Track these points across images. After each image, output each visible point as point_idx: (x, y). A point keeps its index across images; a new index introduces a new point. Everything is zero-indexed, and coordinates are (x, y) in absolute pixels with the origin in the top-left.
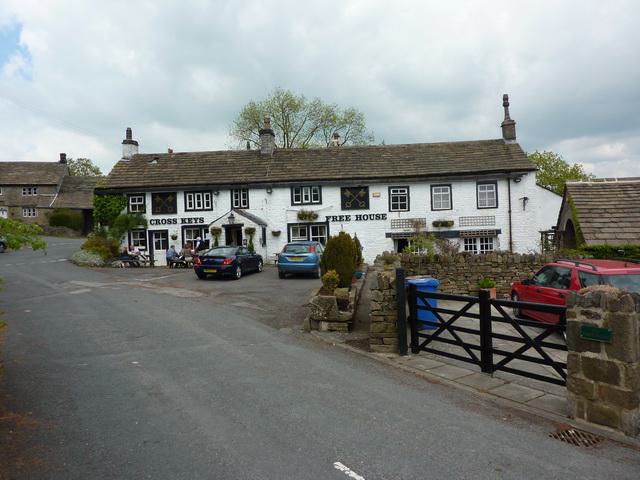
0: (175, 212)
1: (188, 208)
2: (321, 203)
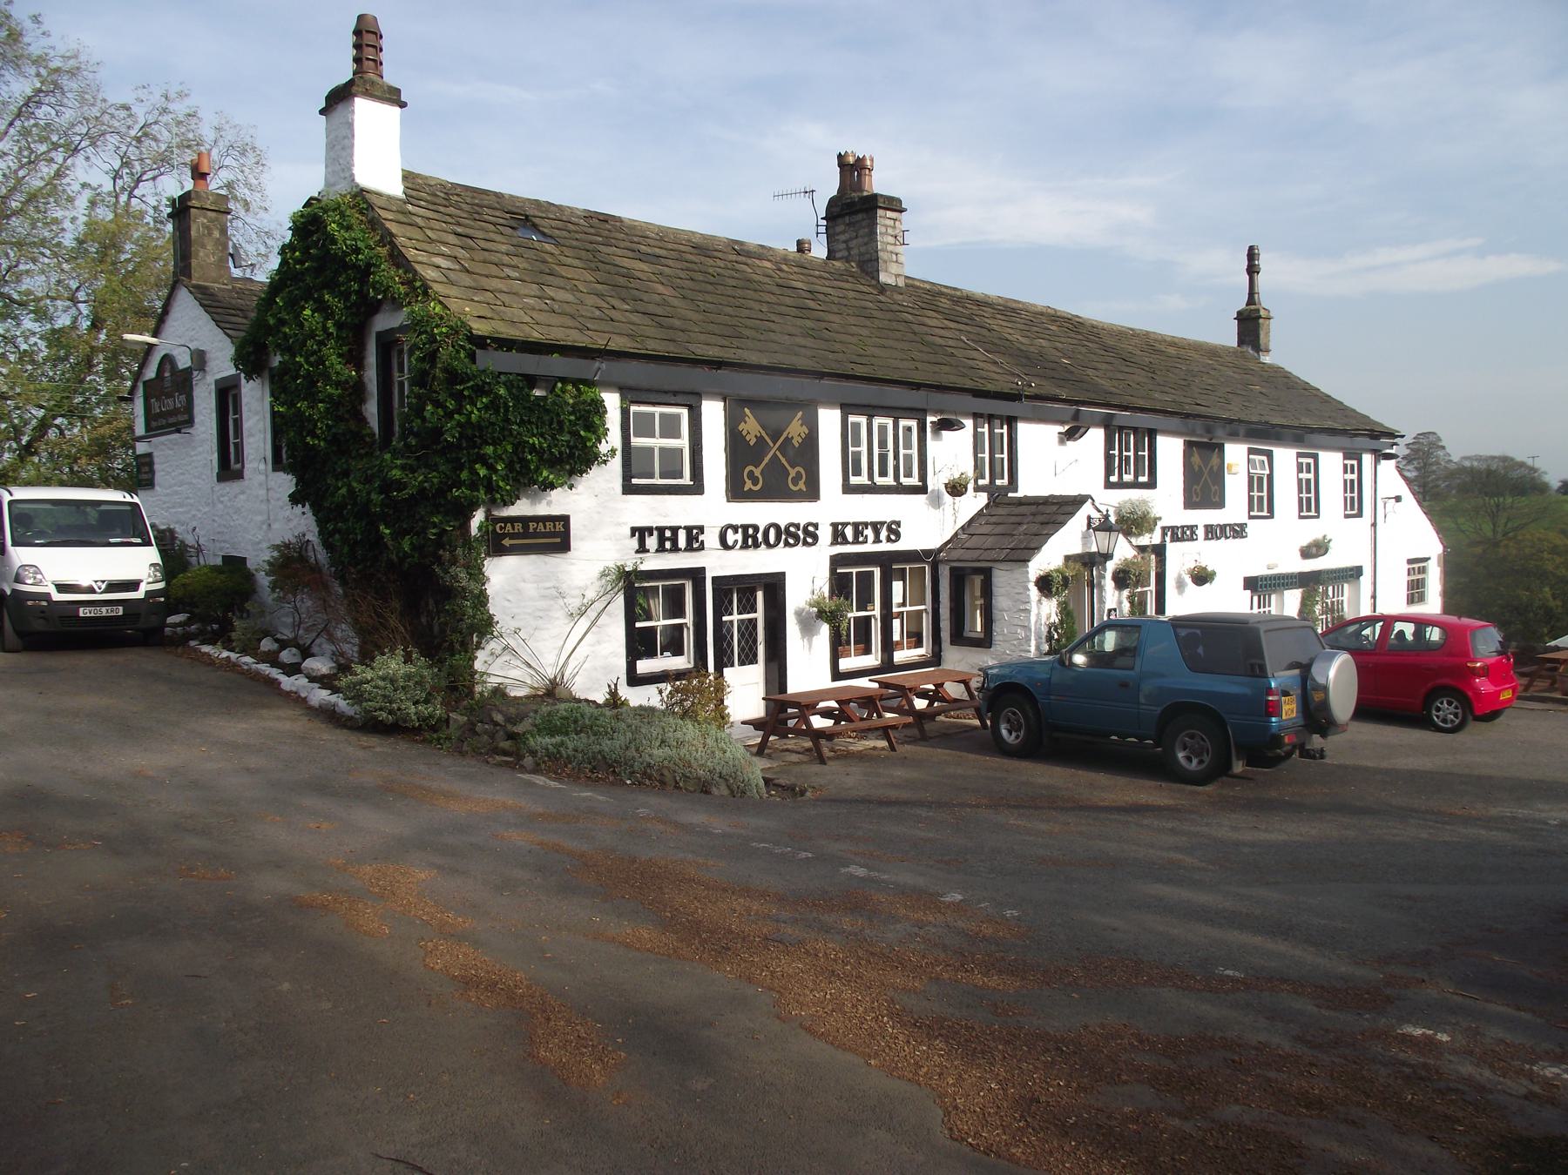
0: (812, 493)
1: (854, 480)
2: (1151, 484)
